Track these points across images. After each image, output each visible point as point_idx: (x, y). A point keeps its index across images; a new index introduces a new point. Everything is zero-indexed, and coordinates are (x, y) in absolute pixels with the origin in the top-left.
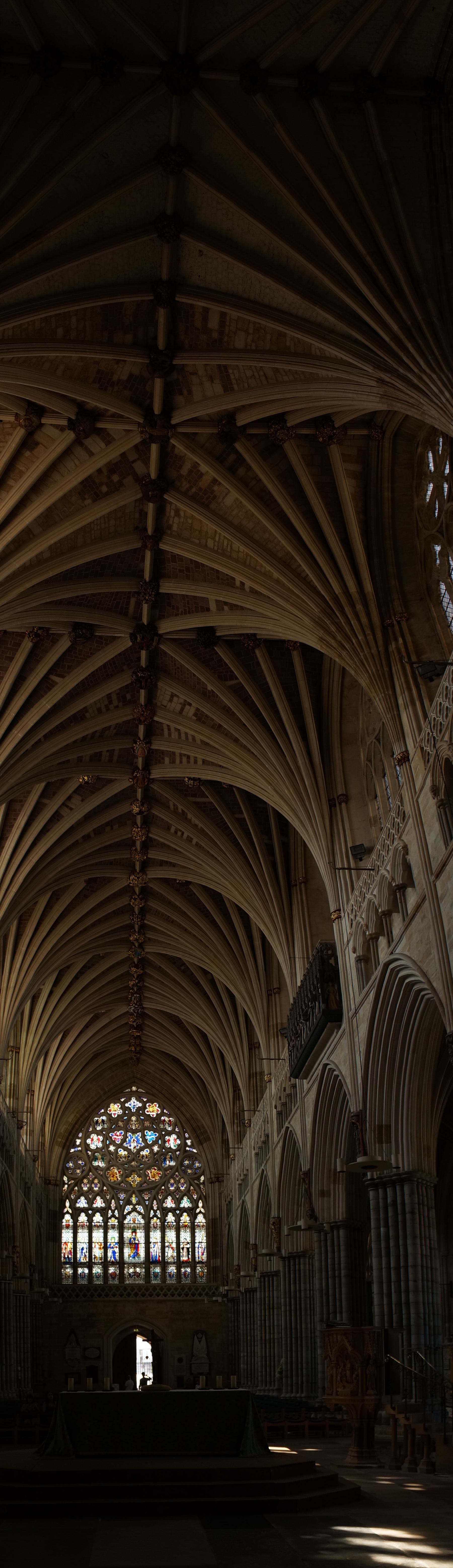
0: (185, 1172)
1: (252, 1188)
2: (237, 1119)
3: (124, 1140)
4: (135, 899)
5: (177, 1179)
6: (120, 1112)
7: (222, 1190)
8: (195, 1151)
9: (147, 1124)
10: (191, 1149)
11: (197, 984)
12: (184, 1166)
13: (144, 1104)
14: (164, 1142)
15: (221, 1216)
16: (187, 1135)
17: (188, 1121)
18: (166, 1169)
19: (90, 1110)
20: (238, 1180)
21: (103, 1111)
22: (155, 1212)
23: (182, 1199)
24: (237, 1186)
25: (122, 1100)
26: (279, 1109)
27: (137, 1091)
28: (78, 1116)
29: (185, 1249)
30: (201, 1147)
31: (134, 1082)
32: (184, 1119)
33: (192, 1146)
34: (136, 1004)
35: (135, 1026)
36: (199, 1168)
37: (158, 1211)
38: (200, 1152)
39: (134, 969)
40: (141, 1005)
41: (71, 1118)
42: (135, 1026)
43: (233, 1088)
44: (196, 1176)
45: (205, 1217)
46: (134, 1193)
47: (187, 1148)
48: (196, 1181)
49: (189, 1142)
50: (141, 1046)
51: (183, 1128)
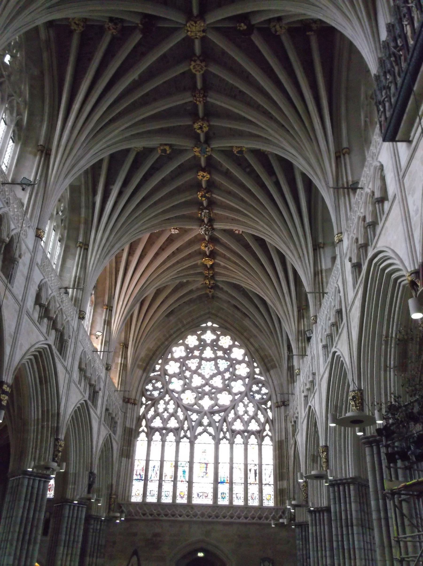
0: (254, 397)
1: (320, 385)
2: (302, 336)
3: (199, 367)
4: (195, 61)
5: (246, 403)
6: (197, 343)
7: (287, 413)
8: (263, 378)
9: (220, 353)
10: (259, 377)
11: (263, 186)
12: (252, 391)
13: (218, 336)
14: (235, 369)
15: (286, 438)
16: (255, 365)
17: (257, 350)
18: (236, 394)
19: (170, 339)
20: (303, 392)
21: (181, 341)
22: (225, 433)
23: (250, 422)
24: (303, 399)
25: (199, 333)
26: (354, 260)
27: (212, 326)
28: (159, 344)
29: (253, 471)
30: (268, 374)
31: (209, 318)
32: (253, 349)
33: (260, 374)
34: (207, 225)
35: (208, 253)
36: (265, 394)
37: (228, 433)
38: (268, 380)
39: (201, 173)
40: (211, 226)
41: (151, 344)
42: (208, 253)
43: (298, 308)
44: (263, 401)
45: (272, 439)
46: (205, 414)
47: (256, 376)
48: (263, 406)
49: (257, 371)
50: (215, 280)
51: (253, 358)
